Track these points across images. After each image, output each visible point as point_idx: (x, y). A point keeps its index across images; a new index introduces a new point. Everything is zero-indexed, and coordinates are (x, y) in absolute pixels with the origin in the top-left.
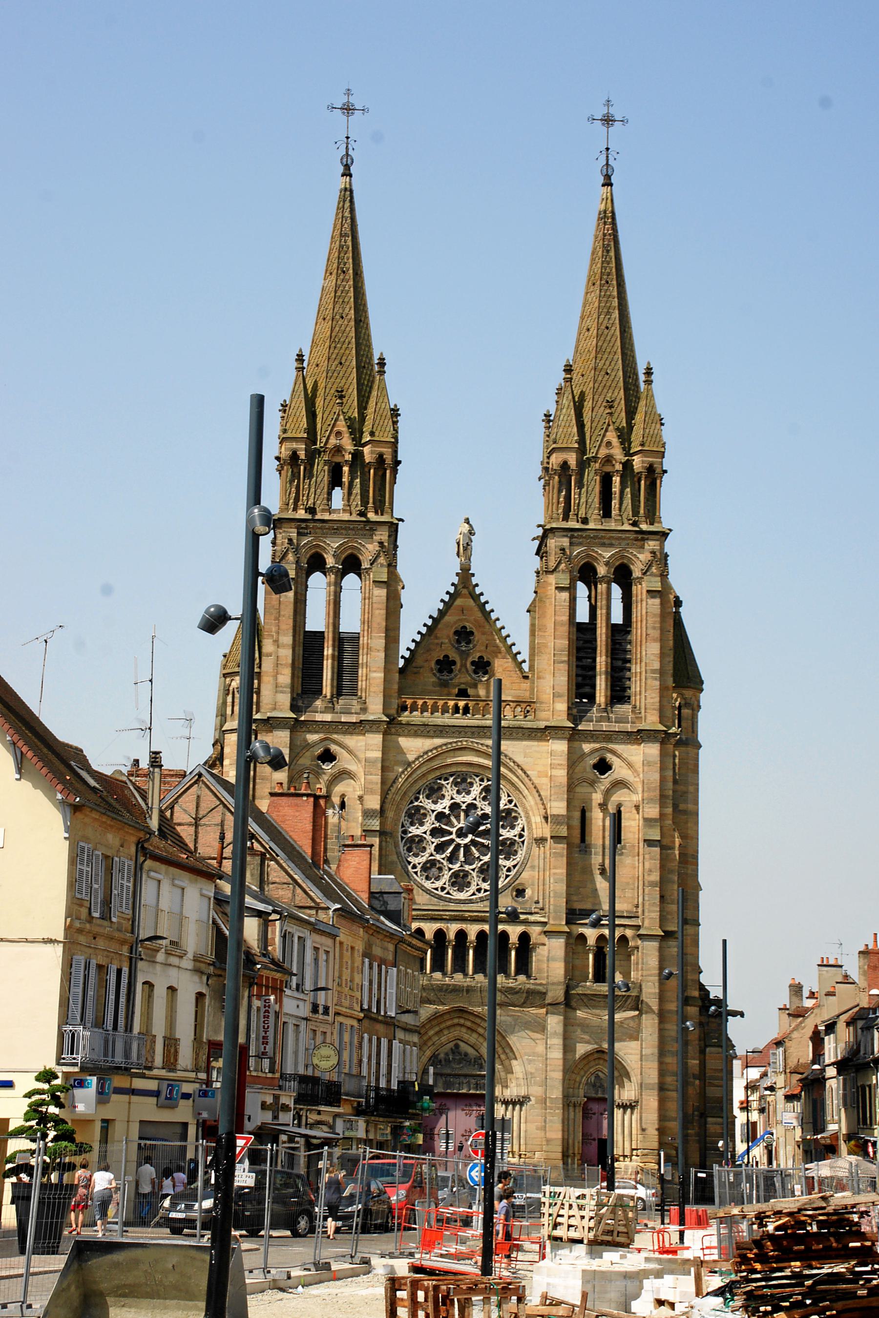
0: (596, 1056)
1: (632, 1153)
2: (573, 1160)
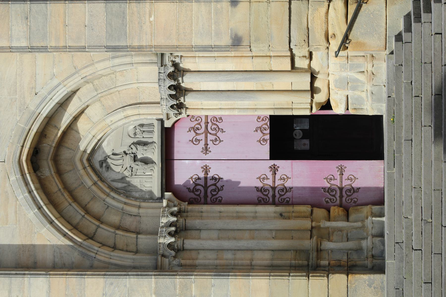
0: (48, 170)
2: (328, 235)
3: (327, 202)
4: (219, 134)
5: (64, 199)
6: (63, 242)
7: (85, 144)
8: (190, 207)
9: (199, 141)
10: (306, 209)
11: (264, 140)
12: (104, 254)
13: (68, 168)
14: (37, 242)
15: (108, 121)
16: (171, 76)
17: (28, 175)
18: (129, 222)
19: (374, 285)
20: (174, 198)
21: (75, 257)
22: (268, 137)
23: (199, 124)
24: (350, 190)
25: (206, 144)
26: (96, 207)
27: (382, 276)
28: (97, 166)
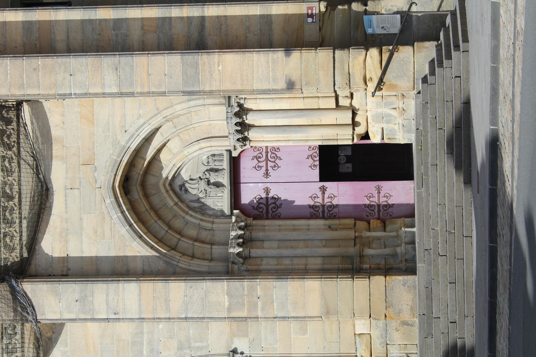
0: (137, 193)
1: (344, 108)
2: (369, 243)
3: (367, 216)
4: (278, 161)
5: (151, 218)
6: (150, 253)
7: (167, 172)
8: (255, 222)
9: (261, 167)
10: (351, 222)
11: (314, 166)
12: (184, 263)
13: (153, 192)
14: (129, 253)
15: (186, 152)
16: (237, 115)
17: (120, 199)
18: (204, 235)
19: (408, 284)
20: (242, 215)
21: (161, 265)
22: (317, 163)
23: (261, 153)
24: (386, 206)
25: (267, 170)
26: (178, 224)
27: (414, 277)
28: (177, 189)
